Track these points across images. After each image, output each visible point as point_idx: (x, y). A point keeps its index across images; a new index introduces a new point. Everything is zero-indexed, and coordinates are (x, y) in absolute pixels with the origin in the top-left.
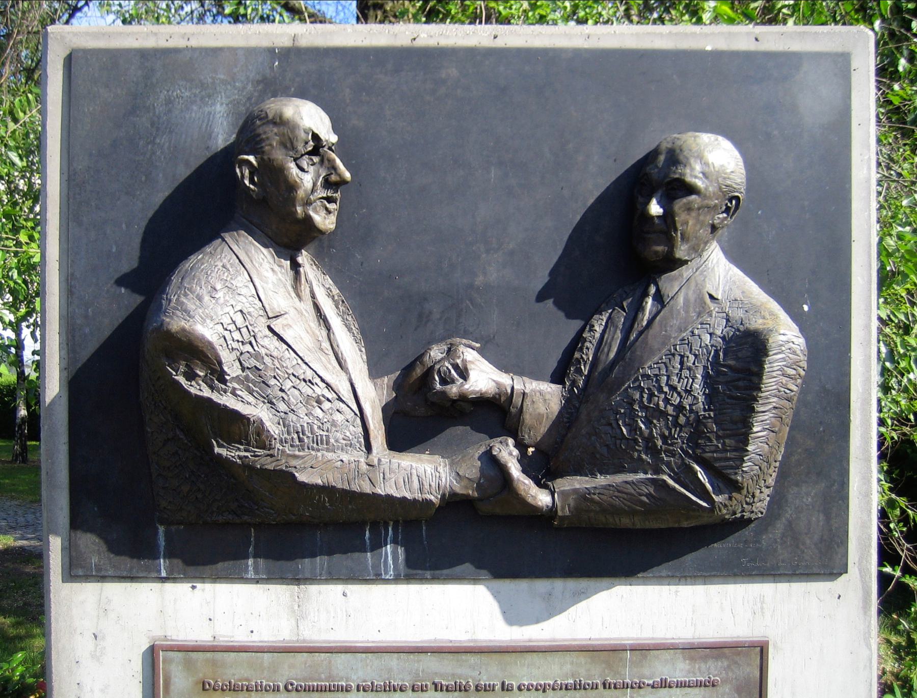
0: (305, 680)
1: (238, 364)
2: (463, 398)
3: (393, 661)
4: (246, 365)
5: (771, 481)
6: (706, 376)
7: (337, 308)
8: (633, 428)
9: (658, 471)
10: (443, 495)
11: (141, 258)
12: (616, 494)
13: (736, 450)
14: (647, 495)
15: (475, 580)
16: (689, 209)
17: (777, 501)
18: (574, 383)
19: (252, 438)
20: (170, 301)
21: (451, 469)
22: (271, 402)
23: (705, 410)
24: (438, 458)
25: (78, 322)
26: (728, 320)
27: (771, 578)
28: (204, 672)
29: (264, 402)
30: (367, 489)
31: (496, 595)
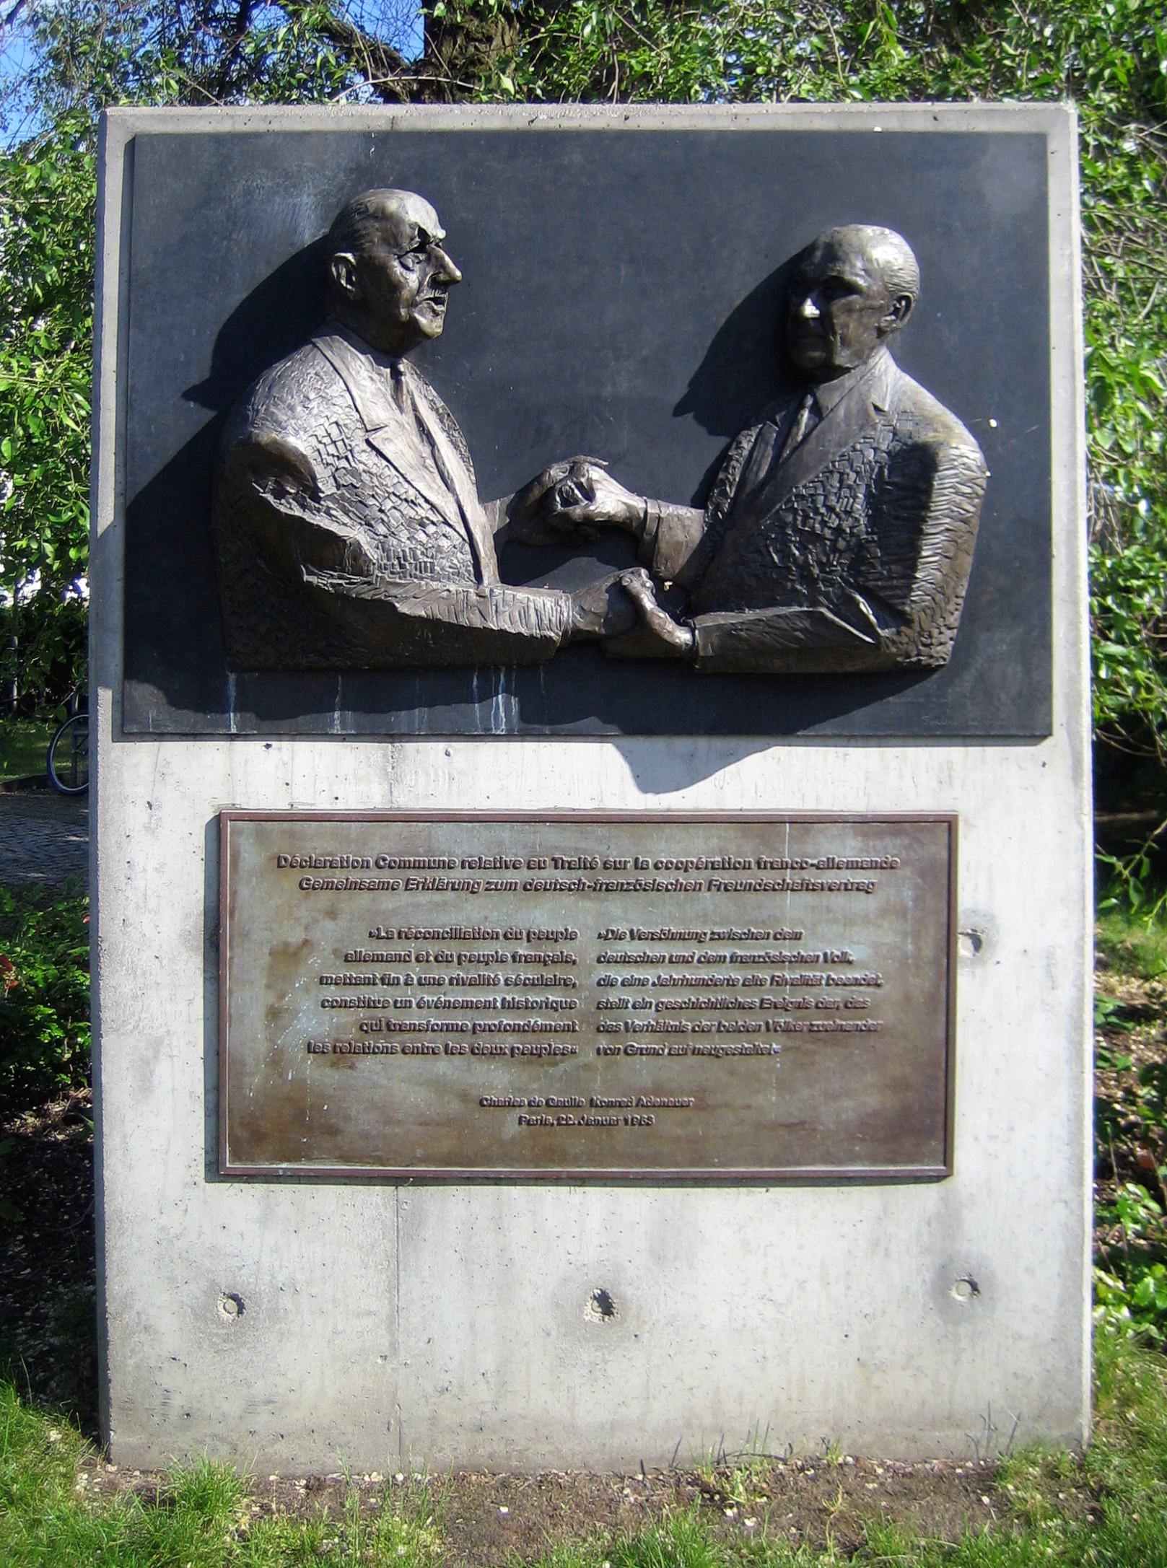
0: (399, 855)
1: (332, 481)
2: (588, 520)
3: (505, 832)
4: (342, 482)
5: (954, 619)
6: (868, 495)
7: (442, 421)
8: (786, 554)
9: (815, 603)
10: (565, 632)
11: (214, 369)
12: (767, 629)
13: (902, 577)
14: (801, 630)
15: (602, 738)
16: (849, 310)
18: (718, 507)
19: (348, 562)
20: (258, 411)
21: (574, 601)
22: (369, 524)
23: (867, 533)
24: (559, 592)
25: (139, 439)
26: (895, 434)
27: (960, 741)
28: (280, 845)
30: (477, 622)
31: (627, 755)
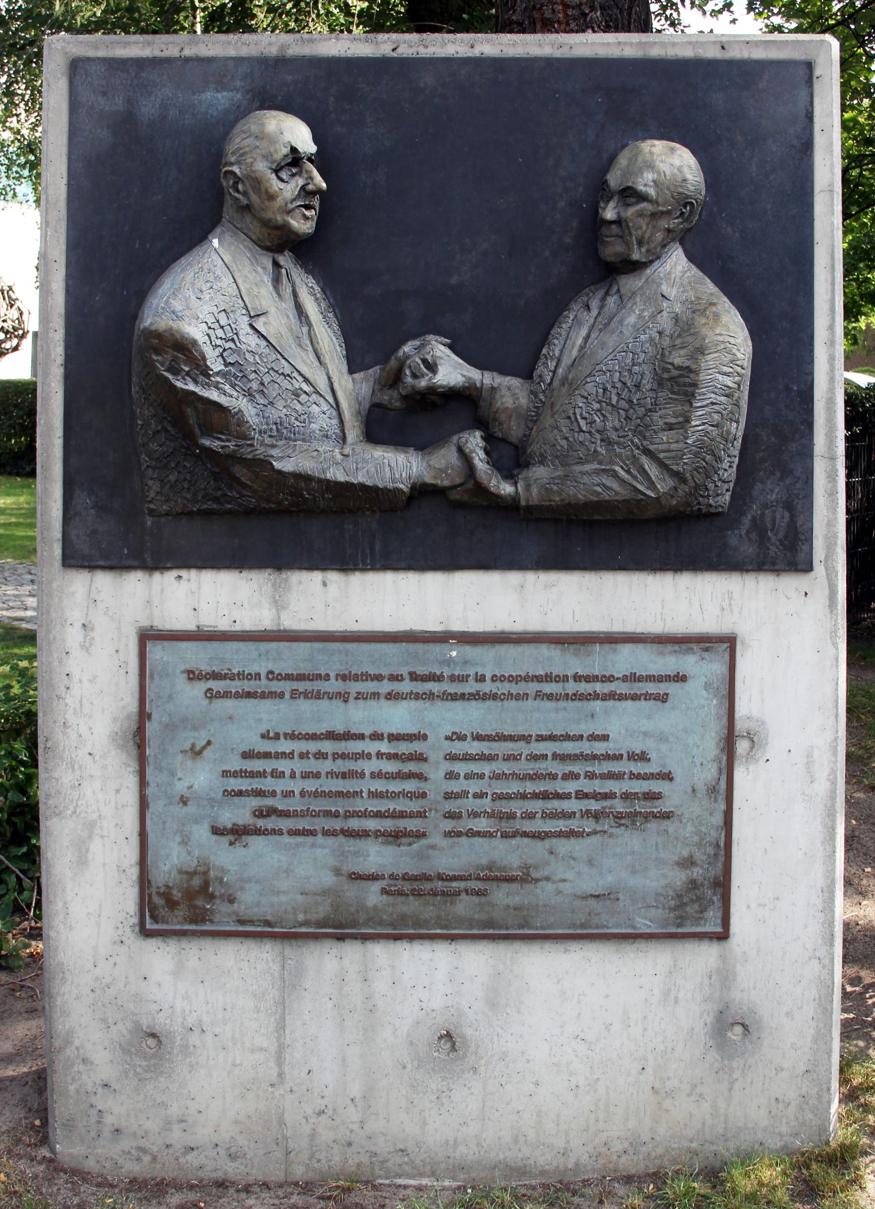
2: (432, 390)
29: (244, 395)
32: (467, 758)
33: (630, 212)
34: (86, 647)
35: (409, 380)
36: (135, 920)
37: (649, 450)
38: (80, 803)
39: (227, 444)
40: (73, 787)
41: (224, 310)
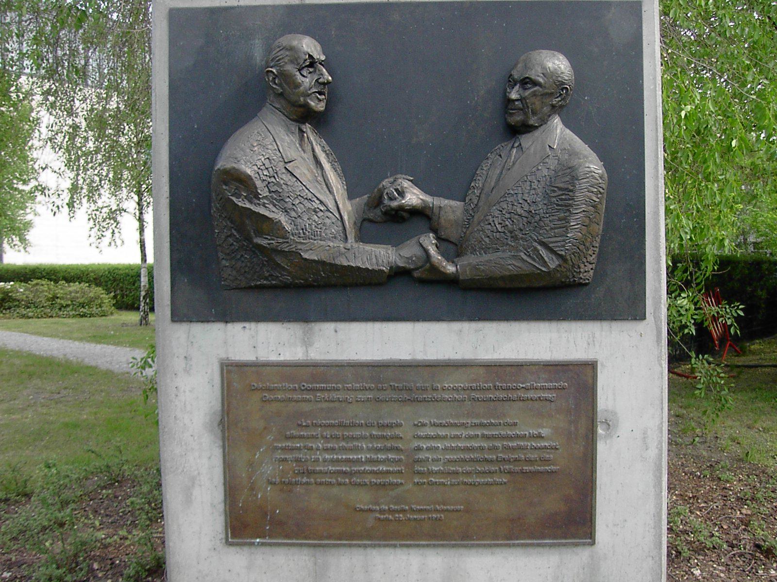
1: (267, 189)
2: (401, 208)
4: (271, 190)
10: (391, 268)
17: (600, 274)
22: (286, 211)
32: (428, 438)
33: (527, 93)
34: (187, 371)
35: (386, 202)
36: (223, 536)
37: (543, 242)
38: (186, 465)
39: (272, 242)
40: (181, 456)
41: (268, 158)
